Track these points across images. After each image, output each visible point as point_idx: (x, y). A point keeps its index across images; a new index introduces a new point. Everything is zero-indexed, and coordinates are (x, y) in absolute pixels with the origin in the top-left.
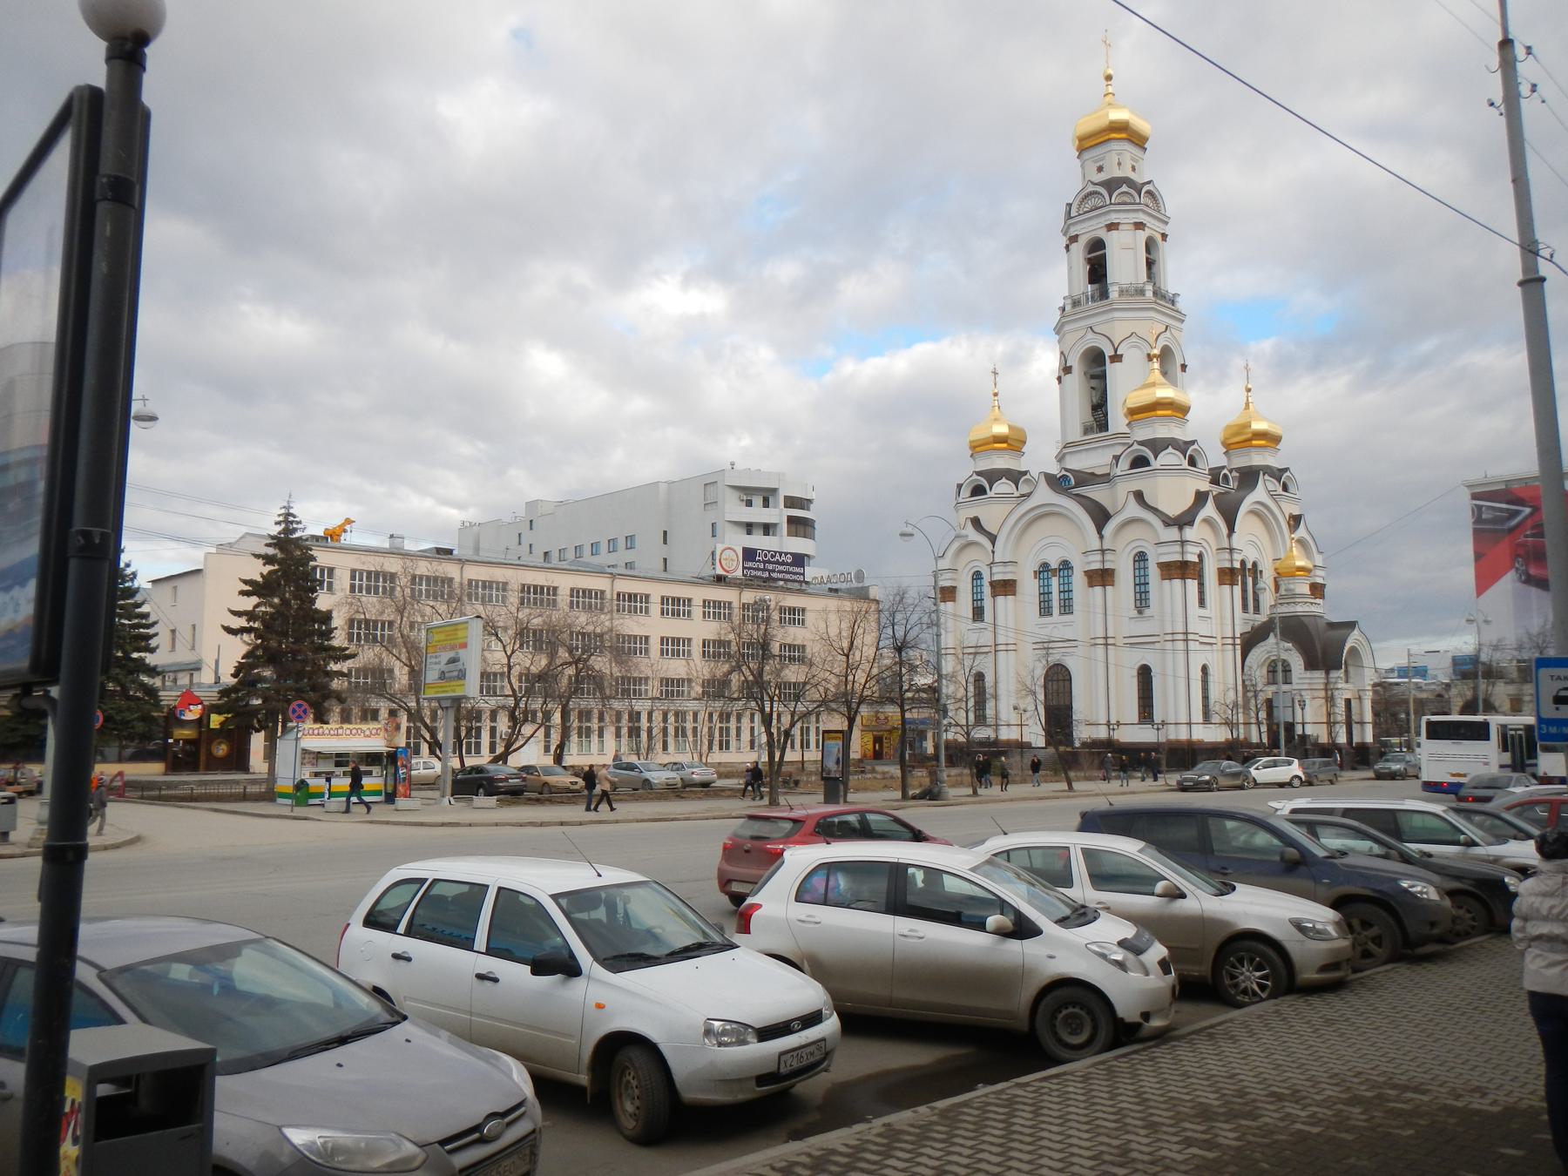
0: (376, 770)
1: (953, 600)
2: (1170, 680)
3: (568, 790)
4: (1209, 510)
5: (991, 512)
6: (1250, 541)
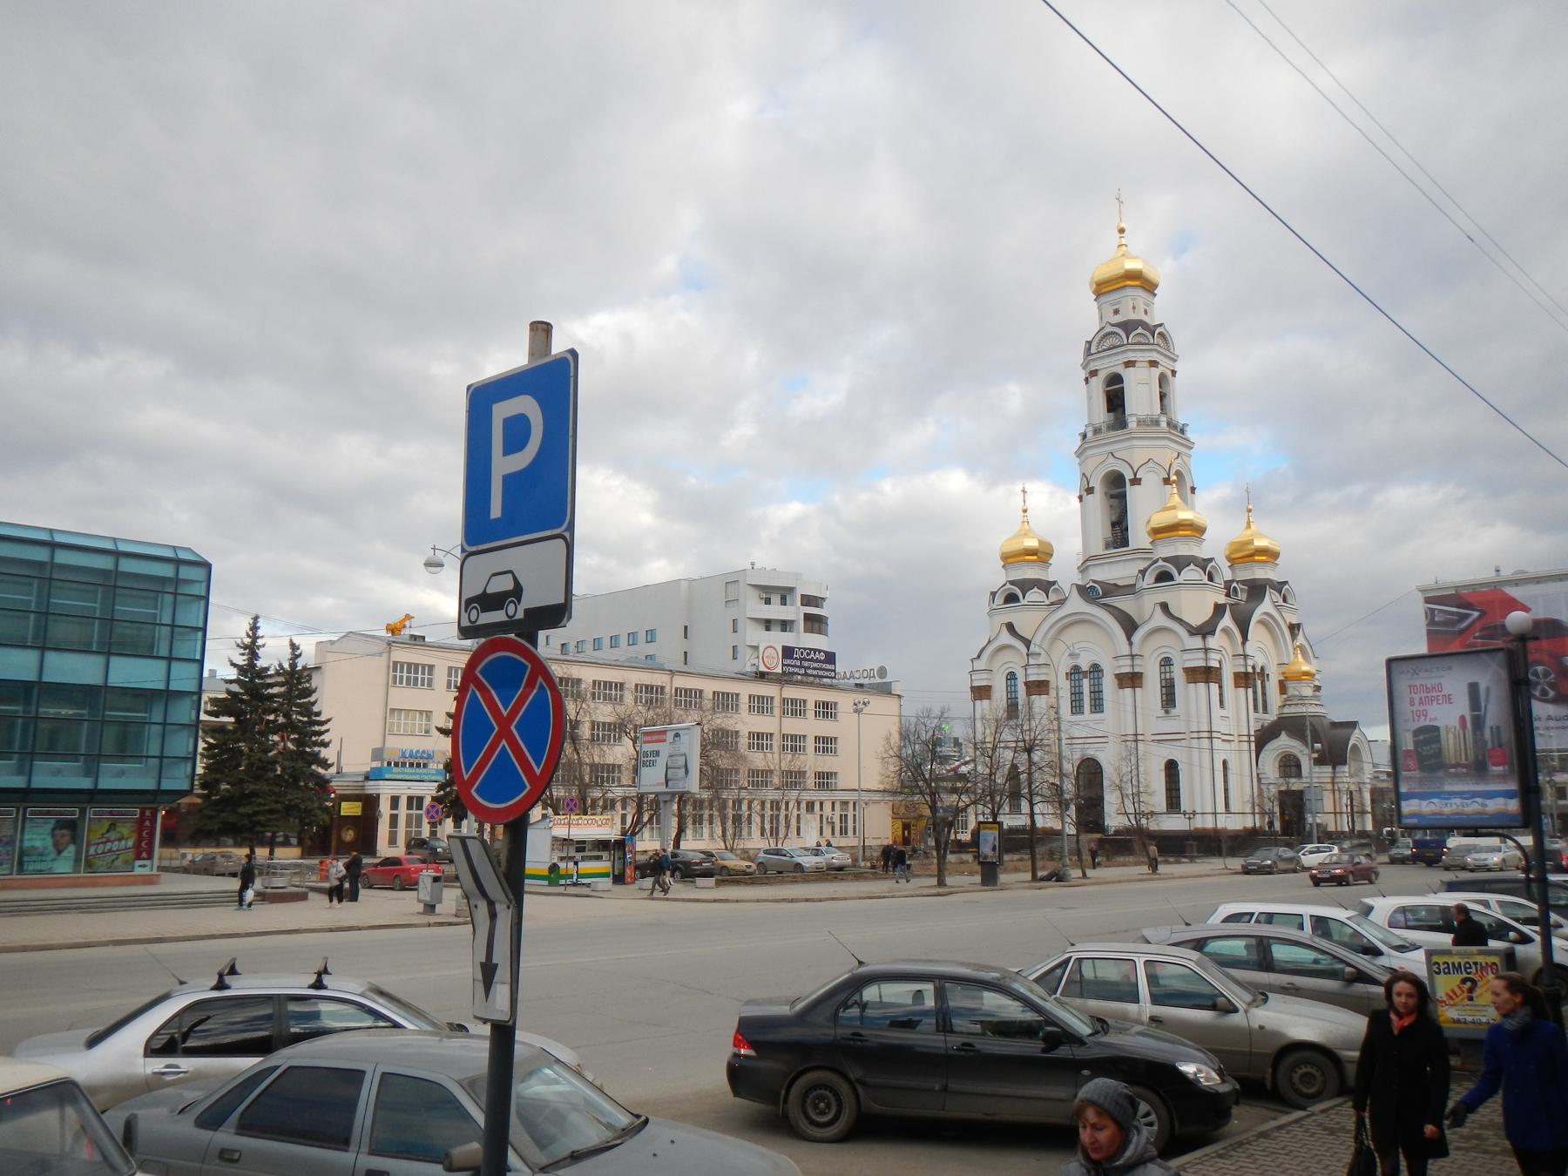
0: (605, 855)
1: (989, 697)
2: (1196, 769)
3: (745, 873)
4: (1227, 621)
5: (1025, 619)
6: (1261, 649)
